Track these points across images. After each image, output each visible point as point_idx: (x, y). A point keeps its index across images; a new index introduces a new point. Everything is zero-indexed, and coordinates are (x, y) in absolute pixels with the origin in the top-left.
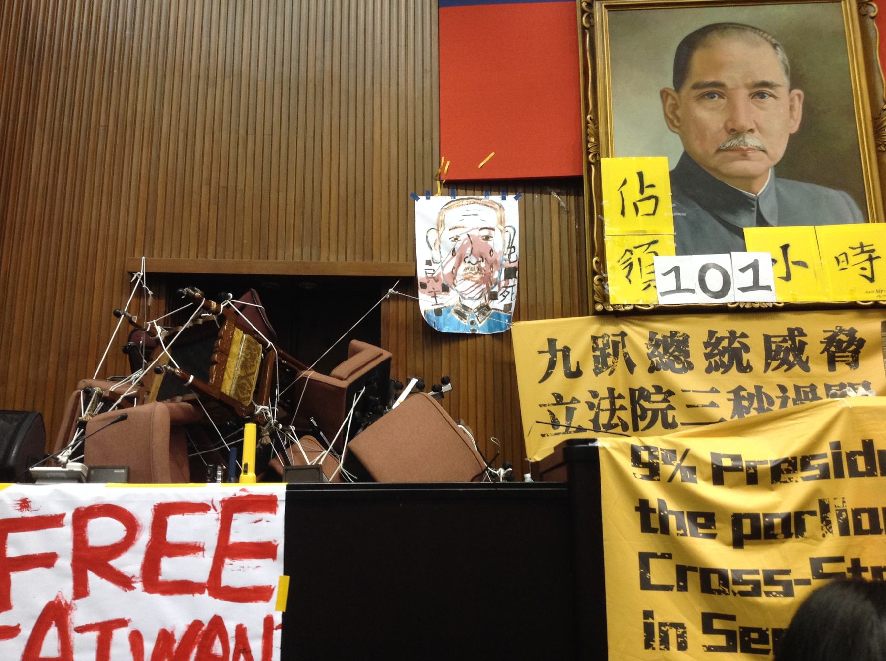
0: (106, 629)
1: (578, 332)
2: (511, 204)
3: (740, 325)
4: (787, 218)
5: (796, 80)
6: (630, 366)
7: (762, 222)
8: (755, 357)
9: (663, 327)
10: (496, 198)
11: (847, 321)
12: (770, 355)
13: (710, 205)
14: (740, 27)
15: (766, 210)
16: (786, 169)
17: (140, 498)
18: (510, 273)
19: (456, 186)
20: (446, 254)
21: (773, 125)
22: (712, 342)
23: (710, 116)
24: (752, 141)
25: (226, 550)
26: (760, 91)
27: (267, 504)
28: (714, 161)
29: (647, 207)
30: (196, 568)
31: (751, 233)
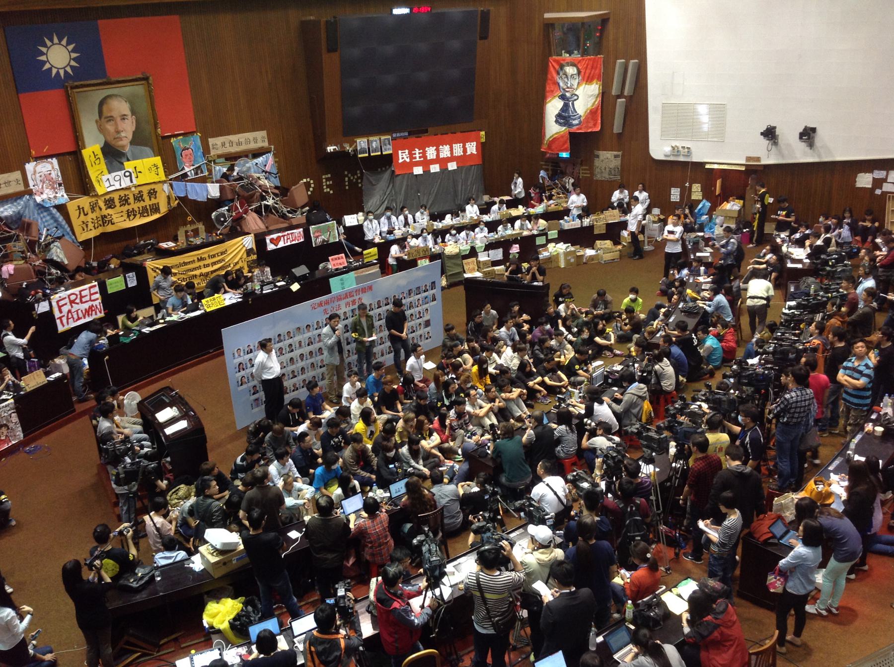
0: (77, 311)
1: (85, 201)
2: (55, 161)
3: (127, 192)
4: (135, 158)
5: (133, 112)
6: (101, 209)
7: (128, 160)
8: (131, 200)
10: (50, 160)
11: (153, 186)
12: (135, 199)
14: (116, 96)
16: (132, 143)
17: (76, 290)
18: (60, 185)
20: (38, 182)
21: (128, 128)
22: (120, 198)
23: (110, 127)
24: (123, 134)
25: (91, 294)
26: (123, 117)
27: (95, 286)
28: (113, 143)
29: (97, 162)
30: (88, 298)
31: (126, 164)
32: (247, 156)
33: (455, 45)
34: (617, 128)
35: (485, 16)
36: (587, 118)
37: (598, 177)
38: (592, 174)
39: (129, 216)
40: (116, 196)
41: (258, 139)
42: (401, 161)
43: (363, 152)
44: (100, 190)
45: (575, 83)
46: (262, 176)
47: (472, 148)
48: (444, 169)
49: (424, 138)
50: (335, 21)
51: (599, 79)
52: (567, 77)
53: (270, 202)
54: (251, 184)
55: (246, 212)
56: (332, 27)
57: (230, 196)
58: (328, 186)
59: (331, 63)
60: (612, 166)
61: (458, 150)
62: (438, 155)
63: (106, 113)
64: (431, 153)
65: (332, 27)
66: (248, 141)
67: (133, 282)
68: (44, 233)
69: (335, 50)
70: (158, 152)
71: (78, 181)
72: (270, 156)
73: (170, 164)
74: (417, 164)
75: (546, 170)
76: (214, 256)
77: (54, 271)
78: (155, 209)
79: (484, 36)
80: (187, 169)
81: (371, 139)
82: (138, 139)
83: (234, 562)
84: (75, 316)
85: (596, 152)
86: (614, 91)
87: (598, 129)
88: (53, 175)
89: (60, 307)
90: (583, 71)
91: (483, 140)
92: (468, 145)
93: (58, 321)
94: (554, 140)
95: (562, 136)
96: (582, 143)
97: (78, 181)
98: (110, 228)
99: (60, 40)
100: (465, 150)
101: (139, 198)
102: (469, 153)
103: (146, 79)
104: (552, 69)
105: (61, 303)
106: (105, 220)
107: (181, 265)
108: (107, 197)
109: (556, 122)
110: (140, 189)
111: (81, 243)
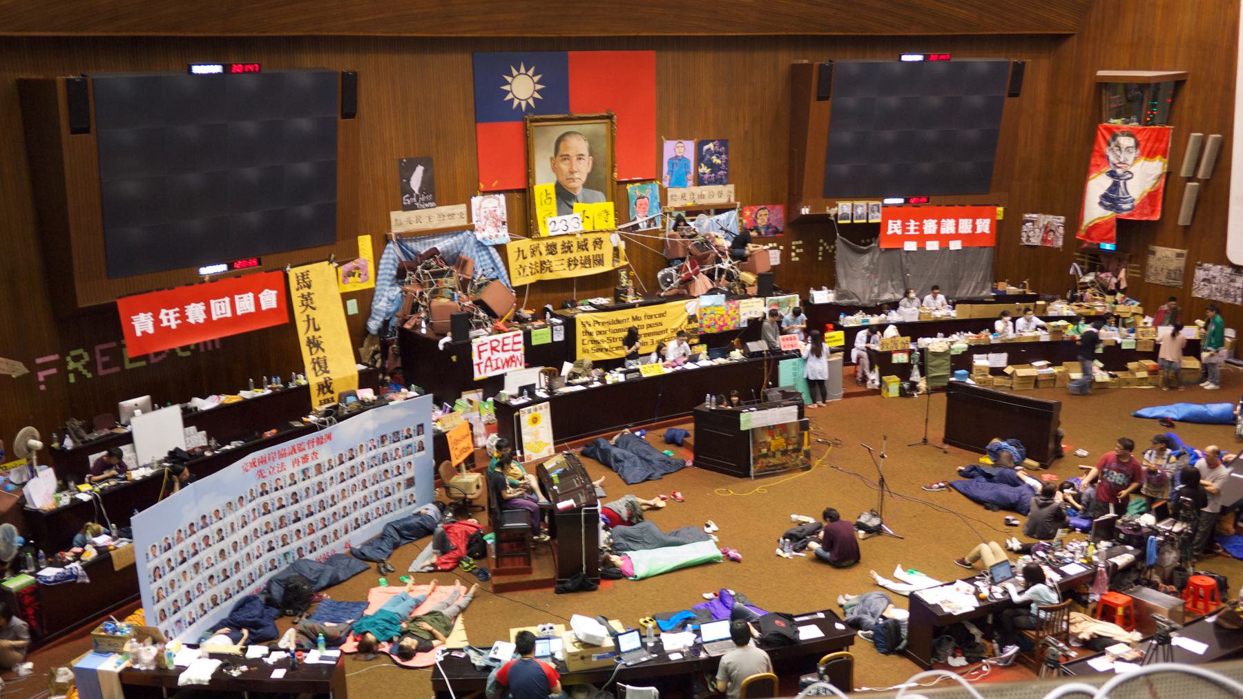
1: (526, 244)
2: (502, 197)
3: (571, 239)
4: (585, 201)
5: (591, 153)
9: (550, 242)
11: (599, 235)
13: (565, 197)
15: (580, 198)
16: (586, 185)
17: (499, 337)
19: (485, 193)
21: (583, 169)
23: (564, 166)
24: (576, 175)
26: (580, 157)
32: (708, 213)
33: (977, 100)
34: (1183, 218)
35: (1019, 70)
36: (1142, 203)
37: (1152, 279)
38: (1144, 274)
39: (569, 265)
40: (559, 242)
41: (722, 193)
42: (890, 232)
43: (845, 217)
44: (543, 232)
45: (1131, 158)
46: (721, 234)
47: (984, 226)
48: (944, 248)
49: (923, 209)
50: (831, 67)
51: (1164, 156)
52: (1120, 150)
53: (726, 265)
54: (707, 242)
55: (696, 273)
56: (826, 73)
57: (681, 255)
58: (797, 255)
59: (819, 112)
60: (1172, 267)
61: (965, 226)
62: (938, 230)
63: (562, 151)
64: (930, 226)
65: (826, 73)
66: (712, 195)
67: (559, 337)
68: (480, 273)
69: (827, 98)
70: (612, 198)
71: (523, 221)
72: (734, 214)
73: (622, 213)
74: (911, 238)
75: (1081, 263)
76: (651, 317)
77: (482, 314)
78: (599, 261)
79: (1014, 94)
80: (639, 220)
81: (856, 203)
82: (592, 183)
83: (594, 659)
84: (494, 363)
85: (1152, 248)
86: (1184, 172)
87: (1157, 217)
88: (498, 213)
89: (480, 352)
90: (1143, 144)
91: (1000, 217)
92: (979, 222)
93: (476, 368)
94: (1095, 227)
95: (1107, 222)
96: (1134, 234)
97: (523, 221)
98: (548, 276)
99: (527, 70)
100: (974, 227)
101: (583, 246)
102: (979, 231)
103: (610, 117)
104: (1101, 139)
105: (482, 348)
106: (543, 266)
107: (613, 323)
108: (550, 242)
109: (1101, 204)
110: (585, 236)
111: (514, 288)
